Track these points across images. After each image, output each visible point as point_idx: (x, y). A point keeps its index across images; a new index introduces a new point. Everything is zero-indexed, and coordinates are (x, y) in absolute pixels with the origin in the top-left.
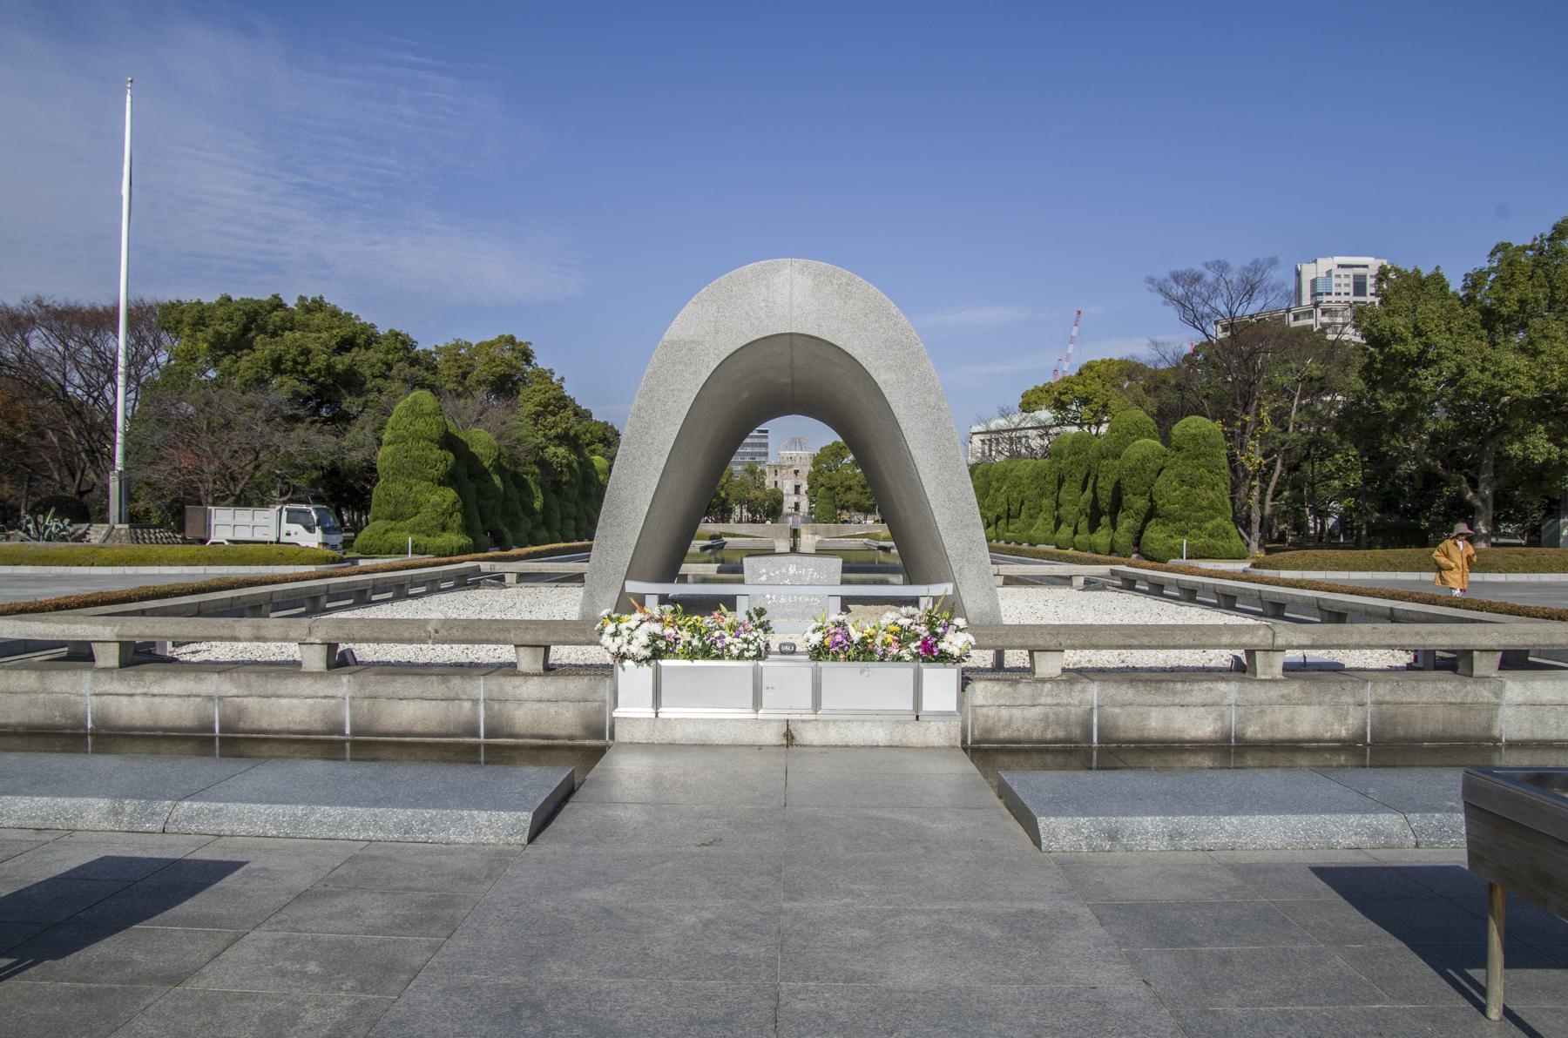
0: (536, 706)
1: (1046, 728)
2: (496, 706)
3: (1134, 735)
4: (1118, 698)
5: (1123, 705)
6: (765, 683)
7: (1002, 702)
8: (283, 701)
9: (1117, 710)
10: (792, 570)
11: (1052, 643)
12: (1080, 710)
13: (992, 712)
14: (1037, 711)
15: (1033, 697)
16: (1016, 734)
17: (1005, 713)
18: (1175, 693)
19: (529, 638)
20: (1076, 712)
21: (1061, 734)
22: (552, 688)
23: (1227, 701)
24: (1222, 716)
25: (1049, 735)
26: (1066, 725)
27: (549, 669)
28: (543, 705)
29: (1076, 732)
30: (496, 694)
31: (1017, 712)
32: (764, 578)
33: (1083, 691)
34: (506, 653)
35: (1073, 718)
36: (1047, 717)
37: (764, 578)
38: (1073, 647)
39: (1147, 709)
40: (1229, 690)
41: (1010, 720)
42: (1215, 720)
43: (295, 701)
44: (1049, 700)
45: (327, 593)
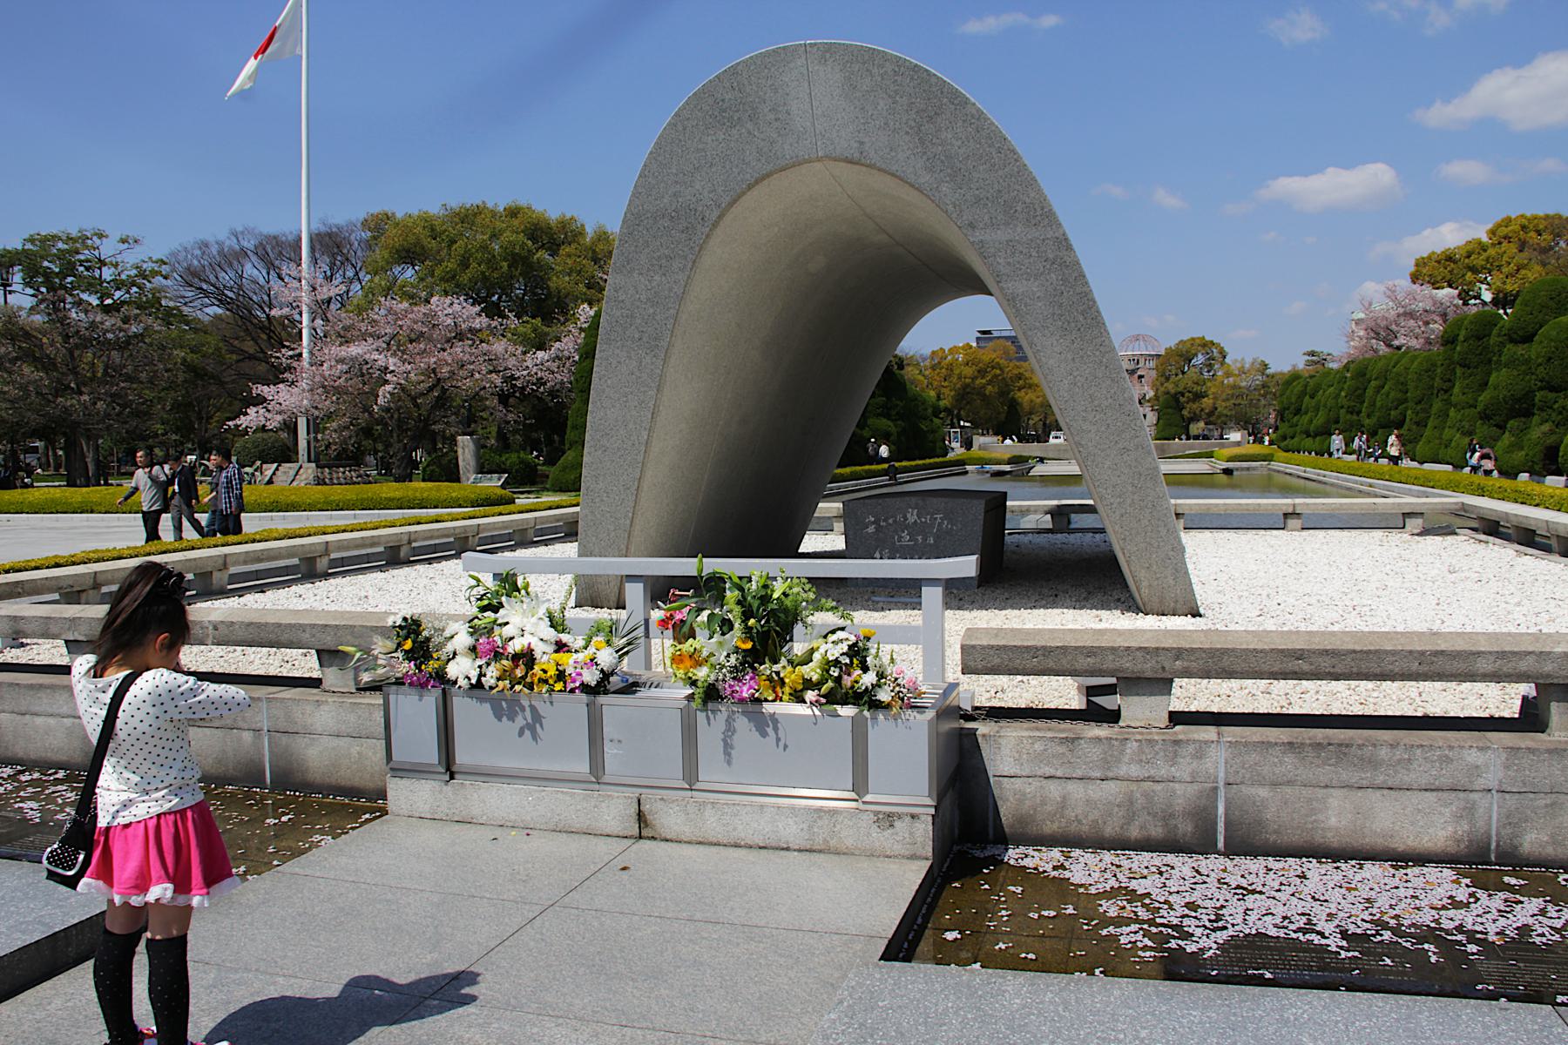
0: (335, 742)
1: (1130, 818)
2: (284, 739)
4: (1266, 770)
5: (1274, 784)
6: (608, 730)
7: (1049, 771)
8: (39, 720)
9: (1263, 792)
10: (912, 517)
11: (1148, 668)
12: (1192, 789)
13: (1031, 788)
14: (1111, 786)
15: (1106, 763)
16: (1074, 828)
17: (1054, 790)
18: (1374, 763)
20: (1184, 795)
22: (352, 718)
23: (1480, 783)
24: (1470, 809)
26: (1167, 817)
28: (343, 743)
29: (1185, 828)
30: (282, 726)
32: (871, 529)
33: (1199, 755)
34: (304, 664)
35: (1180, 804)
37: (871, 529)
38: (1187, 674)
39: (1320, 792)
40: (1486, 758)
41: (1064, 803)
42: (1458, 818)
43: (52, 721)
44: (1135, 771)
45: (327, 552)
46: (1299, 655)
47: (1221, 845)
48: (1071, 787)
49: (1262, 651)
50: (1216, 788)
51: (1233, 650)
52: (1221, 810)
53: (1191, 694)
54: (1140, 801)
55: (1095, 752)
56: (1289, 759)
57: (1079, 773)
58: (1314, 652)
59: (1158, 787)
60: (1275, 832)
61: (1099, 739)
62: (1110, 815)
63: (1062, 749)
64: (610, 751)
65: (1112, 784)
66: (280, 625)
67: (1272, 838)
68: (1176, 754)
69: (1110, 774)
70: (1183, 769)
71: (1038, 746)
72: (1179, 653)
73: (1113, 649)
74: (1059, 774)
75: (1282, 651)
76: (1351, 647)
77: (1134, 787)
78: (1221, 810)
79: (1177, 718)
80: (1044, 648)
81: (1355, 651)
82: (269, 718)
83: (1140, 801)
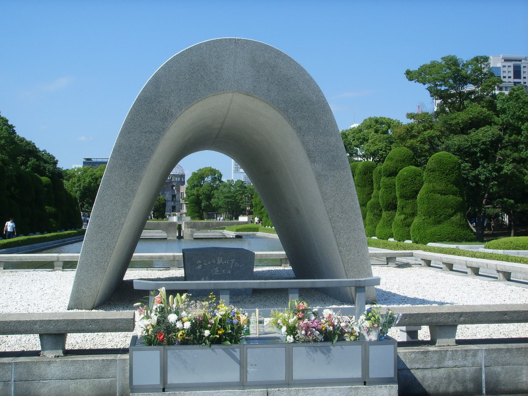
0: (58, 383)
1: (449, 383)
3: (512, 387)
10: (219, 262)
11: (450, 320)
15: (440, 361)
19: (52, 329)
20: (469, 371)
21: (459, 388)
22: (72, 369)
25: (451, 389)
27: (68, 353)
28: (64, 383)
29: (470, 386)
31: (428, 374)
32: (199, 267)
36: (449, 376)
37: (199, 267)
38: (464, 322)
44: (450, 363)
46: (505, 313)
47: (484, 392)
48: (426, 372)
49: (492, 312)
50: (481, 368)
51: (482, 312)
52: (484, 377)
53: (465, 331)
54: (453, 376)
55: (436, 357)
56: (508, 355)
57: (429, 366)
58: (511, 312)
59: (459, 369)
60: (504, 385)
61: (436, 351)
62: (442, 383)
63: (422, 356)
64: (250, 369)
65: (442, 369)
66: (19, 322)
67: (503, 388)
68: (466, 356)
69: (441, 366)
70: (470, 360)
71: (413, 356)
72: (461, 314)
73: (437, 314)
74: (421, 367)
75: (500, 312)
76: (523, 310)
77: (450, 370)
78: (484, 377)
79: (459, 342)
80: (410, 314)
81: (525, 311)
82: (15, 374)
83: (453, 376)
